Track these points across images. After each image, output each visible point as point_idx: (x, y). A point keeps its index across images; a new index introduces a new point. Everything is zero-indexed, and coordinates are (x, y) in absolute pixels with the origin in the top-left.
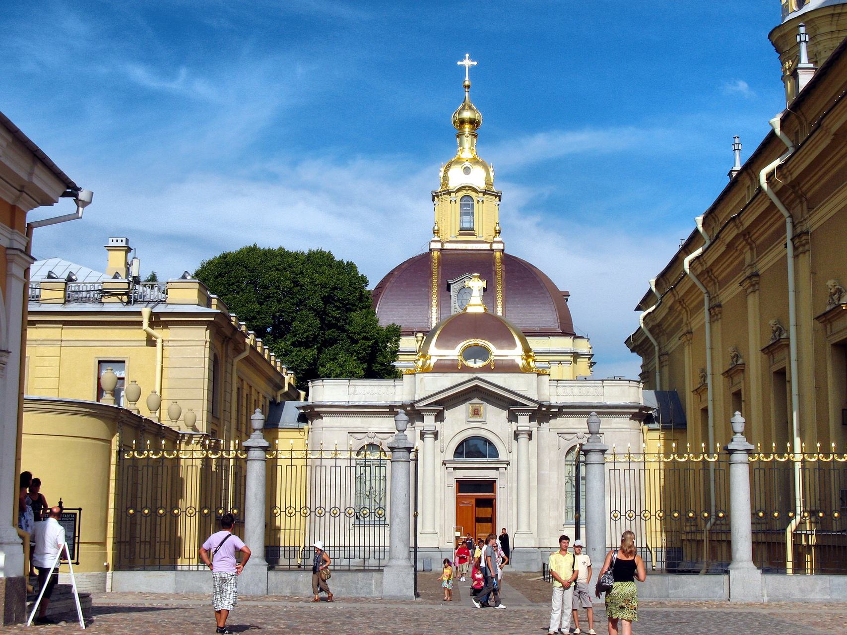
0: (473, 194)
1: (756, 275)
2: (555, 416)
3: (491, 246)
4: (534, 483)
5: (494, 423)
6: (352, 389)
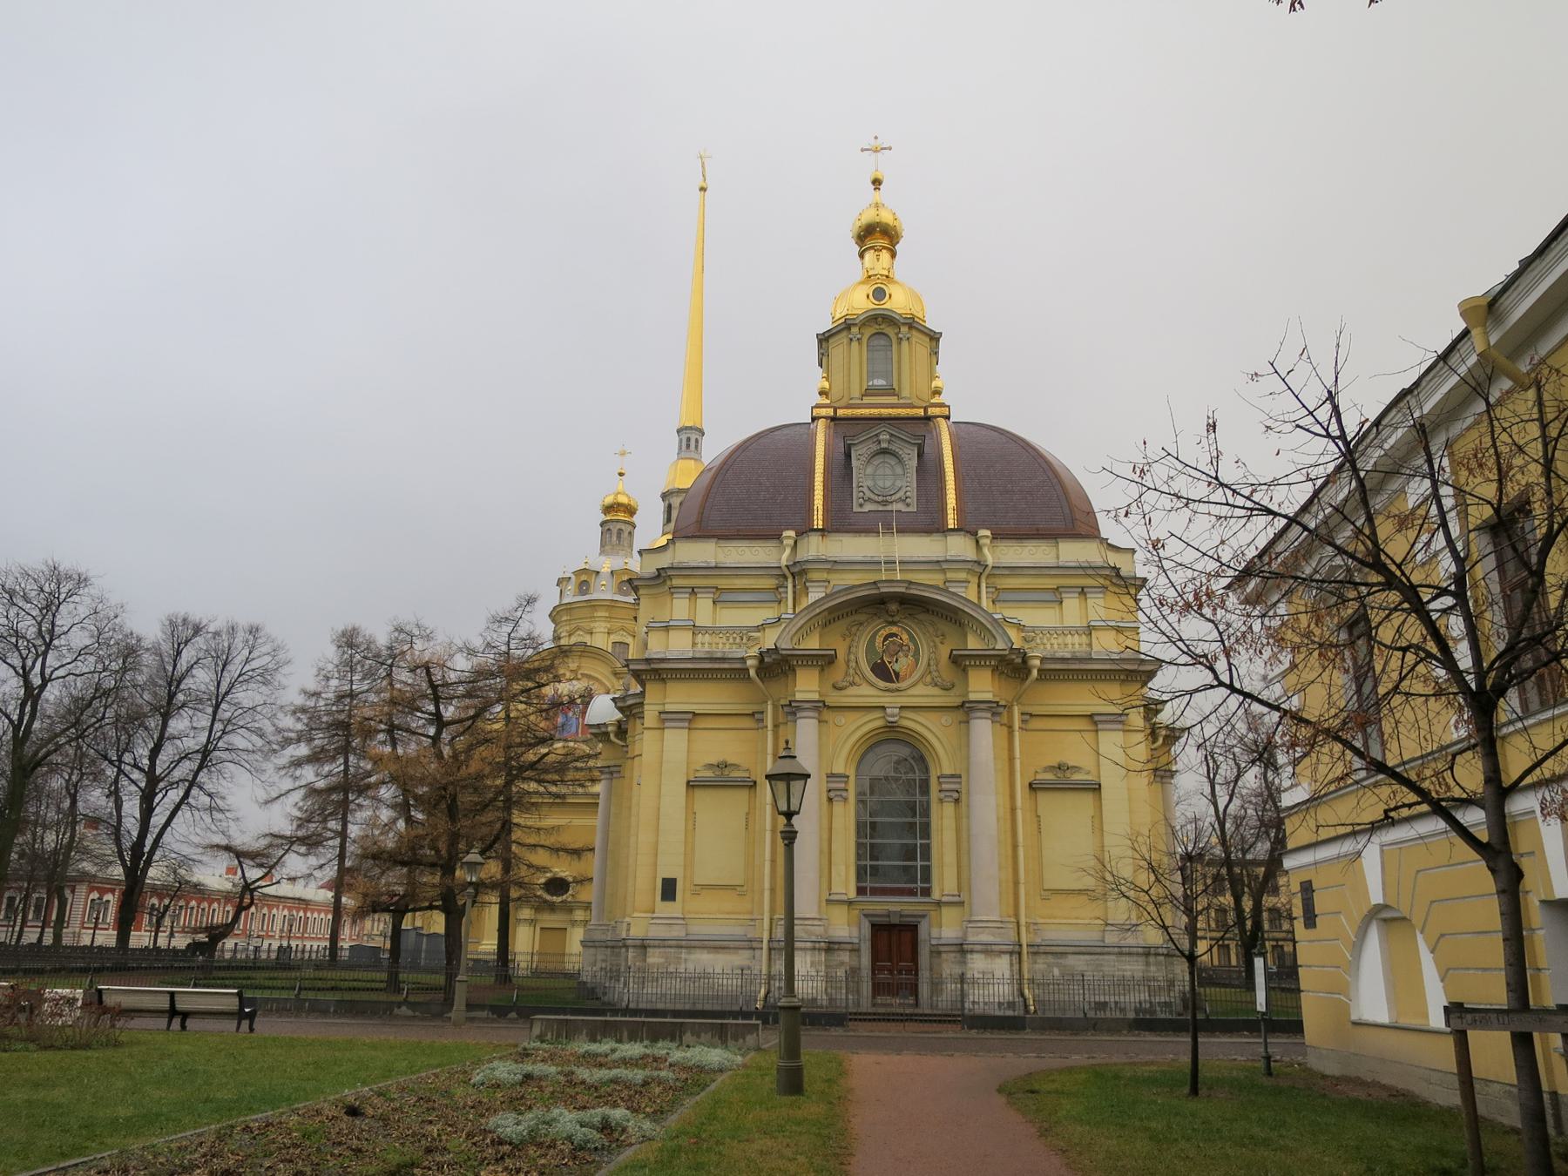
0: (890, 331)
3: (926, 409)
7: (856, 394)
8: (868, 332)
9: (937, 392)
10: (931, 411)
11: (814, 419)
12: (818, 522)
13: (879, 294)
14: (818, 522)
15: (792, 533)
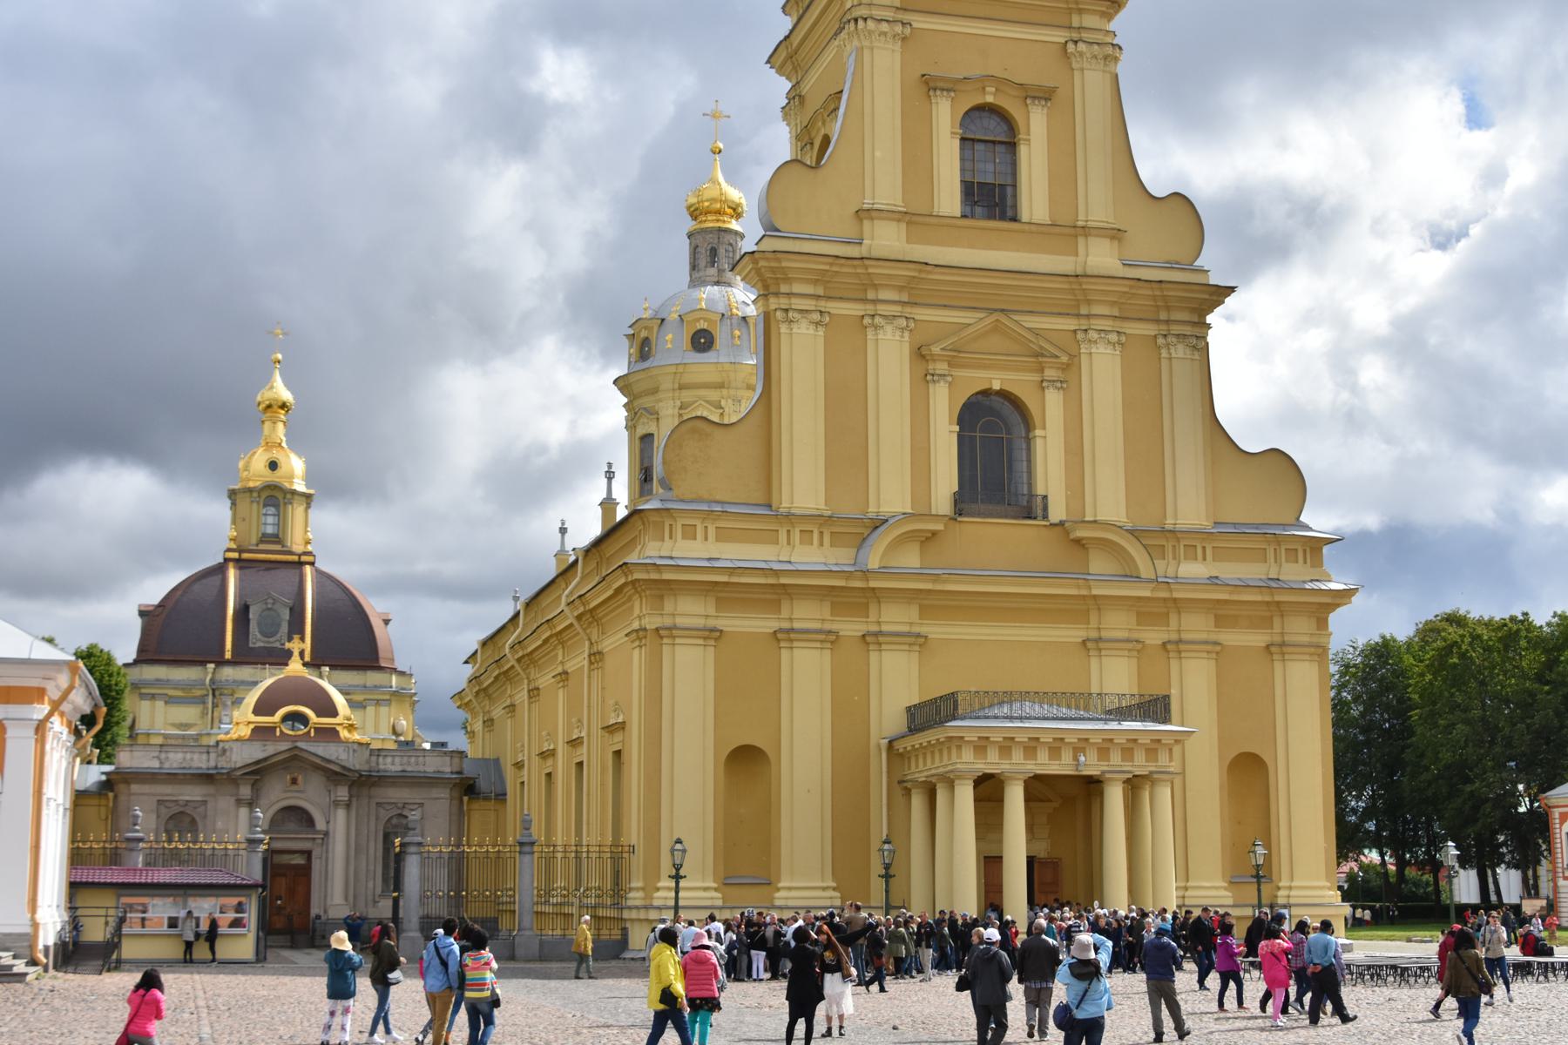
1: (565, 673)
2: (374, 785)
4: (352, 853)
5: (312, 796)
6: (163, 756)
7: (254, 541)
8: (264, 495)
9: (308, 542)
10: (304, 558)
11: (226, 560)
12: (228, 655)
13: (273, 465)
14: (228, 655)
15: (212, 666)
